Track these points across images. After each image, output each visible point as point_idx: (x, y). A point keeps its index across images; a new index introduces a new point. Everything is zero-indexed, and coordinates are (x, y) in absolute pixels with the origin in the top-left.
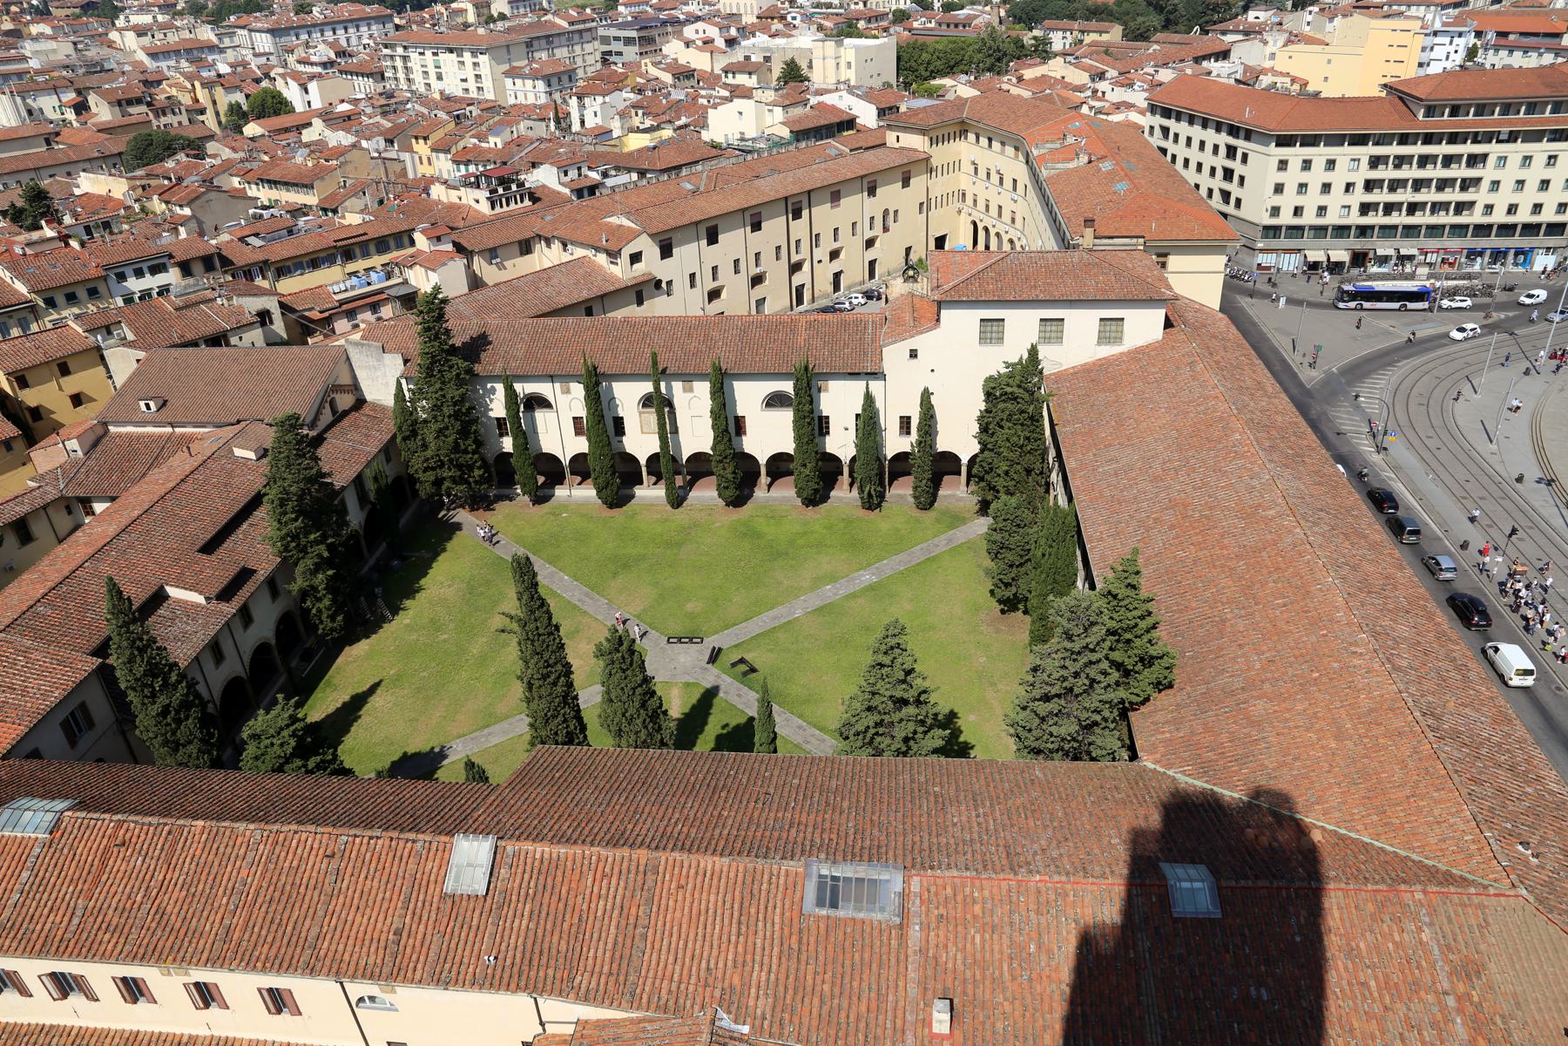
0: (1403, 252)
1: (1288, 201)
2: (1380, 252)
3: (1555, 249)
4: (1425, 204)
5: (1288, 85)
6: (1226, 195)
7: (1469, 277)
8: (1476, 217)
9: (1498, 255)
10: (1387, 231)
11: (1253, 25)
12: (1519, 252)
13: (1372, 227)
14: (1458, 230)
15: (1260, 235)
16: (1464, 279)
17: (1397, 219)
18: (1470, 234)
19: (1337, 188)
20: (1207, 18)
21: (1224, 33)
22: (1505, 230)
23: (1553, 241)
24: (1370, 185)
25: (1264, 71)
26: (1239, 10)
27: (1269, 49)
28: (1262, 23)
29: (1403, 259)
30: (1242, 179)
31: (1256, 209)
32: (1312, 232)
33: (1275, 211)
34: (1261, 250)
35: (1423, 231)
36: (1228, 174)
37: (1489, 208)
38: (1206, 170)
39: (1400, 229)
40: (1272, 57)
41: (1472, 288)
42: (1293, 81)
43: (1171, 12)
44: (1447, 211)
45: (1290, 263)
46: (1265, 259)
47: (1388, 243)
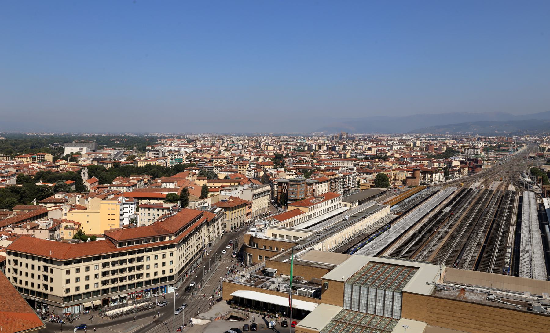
0: (122, 296)
1: (72, 286)
2: (113, 298)
3: (173, 284)
4: (126, 277)
5: (73, 226)
6: (46, 287)
7: (147, 300)
8: (145, 278)
9: (155, 290)
10: (114, 289)
11: (57, 200)
12: (162, 288)
13: (108, 289)
14: (140, 284)
15: (63, 301)
16: (145, 302)
17: (117, 284)
18: (144, 285)
19: (92, 277)
20: (39, 195)
21: (46, 203)
22: (156, 281)
23: (172, 282)
24: (104, 274)
25: (63, 221)
26: (53, 192)
27: (64, 212)
28: (61, 199)
29: (122, 299)
30: (52, 279)
31: (59, 290)
32: (85, 296)
33: (68, 290)
34: (64, 307)
35: (127, 287)
36: (46, 278)
37: (148, 275)
38: (36, 276)
39: (119, 288)
40: (65, 215)
41: (148, 306)
42: (75, 224)
43: (22, 193)
44: (134, 278)
45: (77, 310)
46: (65, 311)
47: (116, 294)
